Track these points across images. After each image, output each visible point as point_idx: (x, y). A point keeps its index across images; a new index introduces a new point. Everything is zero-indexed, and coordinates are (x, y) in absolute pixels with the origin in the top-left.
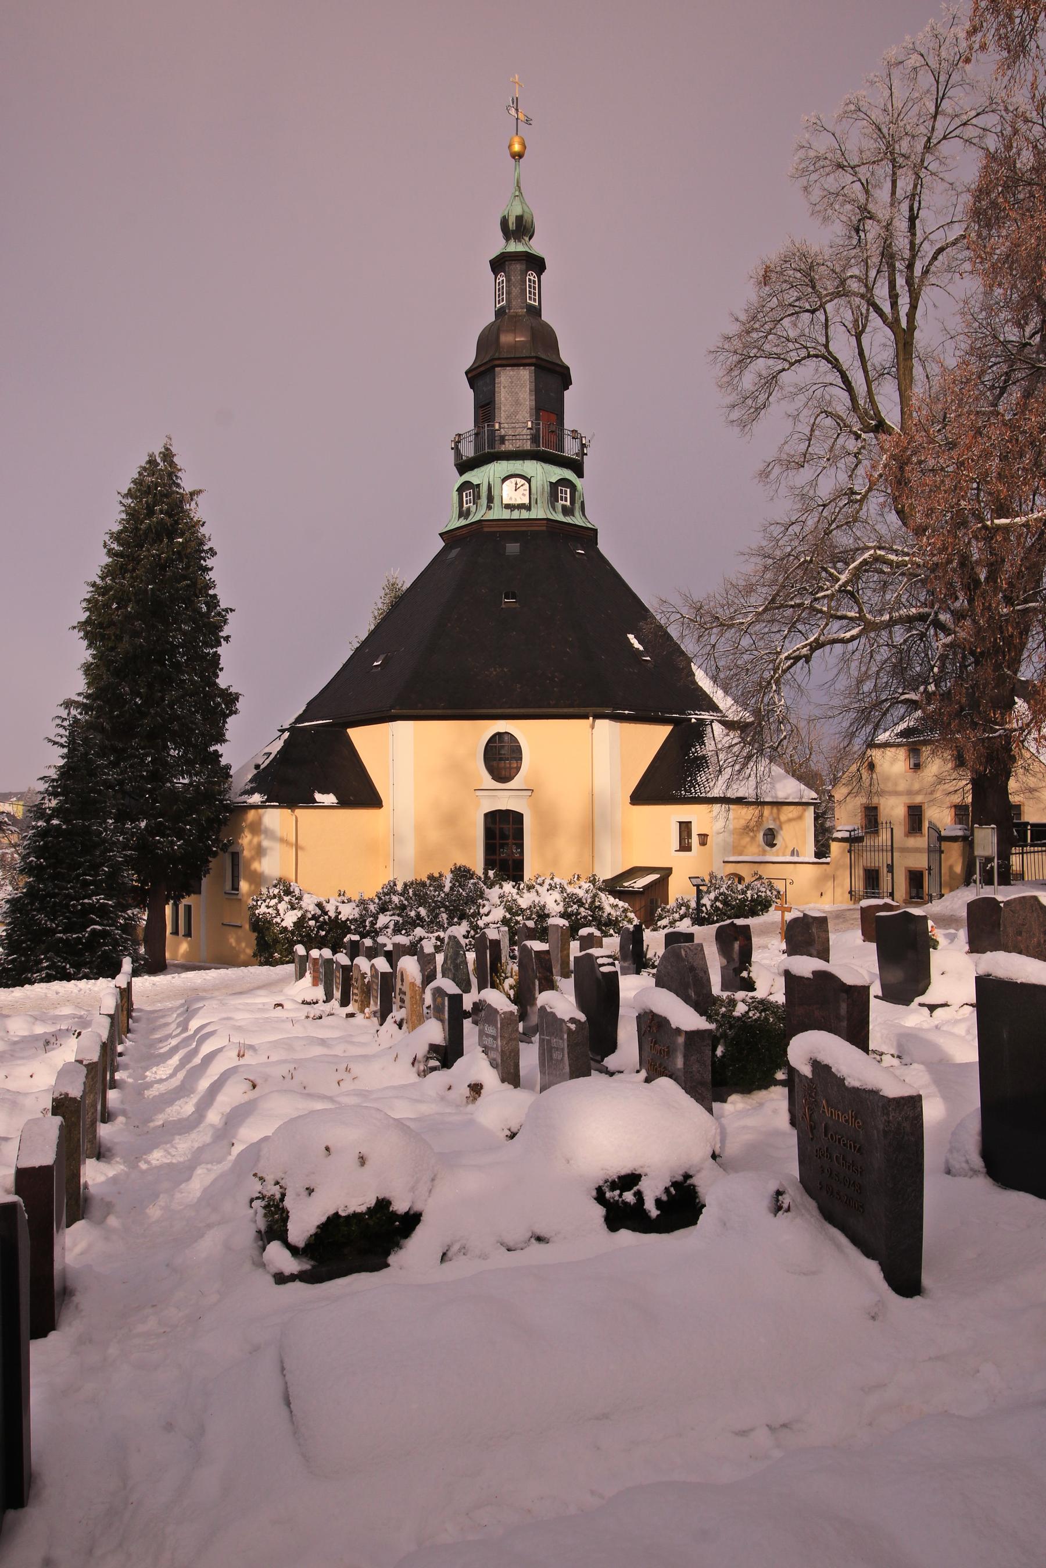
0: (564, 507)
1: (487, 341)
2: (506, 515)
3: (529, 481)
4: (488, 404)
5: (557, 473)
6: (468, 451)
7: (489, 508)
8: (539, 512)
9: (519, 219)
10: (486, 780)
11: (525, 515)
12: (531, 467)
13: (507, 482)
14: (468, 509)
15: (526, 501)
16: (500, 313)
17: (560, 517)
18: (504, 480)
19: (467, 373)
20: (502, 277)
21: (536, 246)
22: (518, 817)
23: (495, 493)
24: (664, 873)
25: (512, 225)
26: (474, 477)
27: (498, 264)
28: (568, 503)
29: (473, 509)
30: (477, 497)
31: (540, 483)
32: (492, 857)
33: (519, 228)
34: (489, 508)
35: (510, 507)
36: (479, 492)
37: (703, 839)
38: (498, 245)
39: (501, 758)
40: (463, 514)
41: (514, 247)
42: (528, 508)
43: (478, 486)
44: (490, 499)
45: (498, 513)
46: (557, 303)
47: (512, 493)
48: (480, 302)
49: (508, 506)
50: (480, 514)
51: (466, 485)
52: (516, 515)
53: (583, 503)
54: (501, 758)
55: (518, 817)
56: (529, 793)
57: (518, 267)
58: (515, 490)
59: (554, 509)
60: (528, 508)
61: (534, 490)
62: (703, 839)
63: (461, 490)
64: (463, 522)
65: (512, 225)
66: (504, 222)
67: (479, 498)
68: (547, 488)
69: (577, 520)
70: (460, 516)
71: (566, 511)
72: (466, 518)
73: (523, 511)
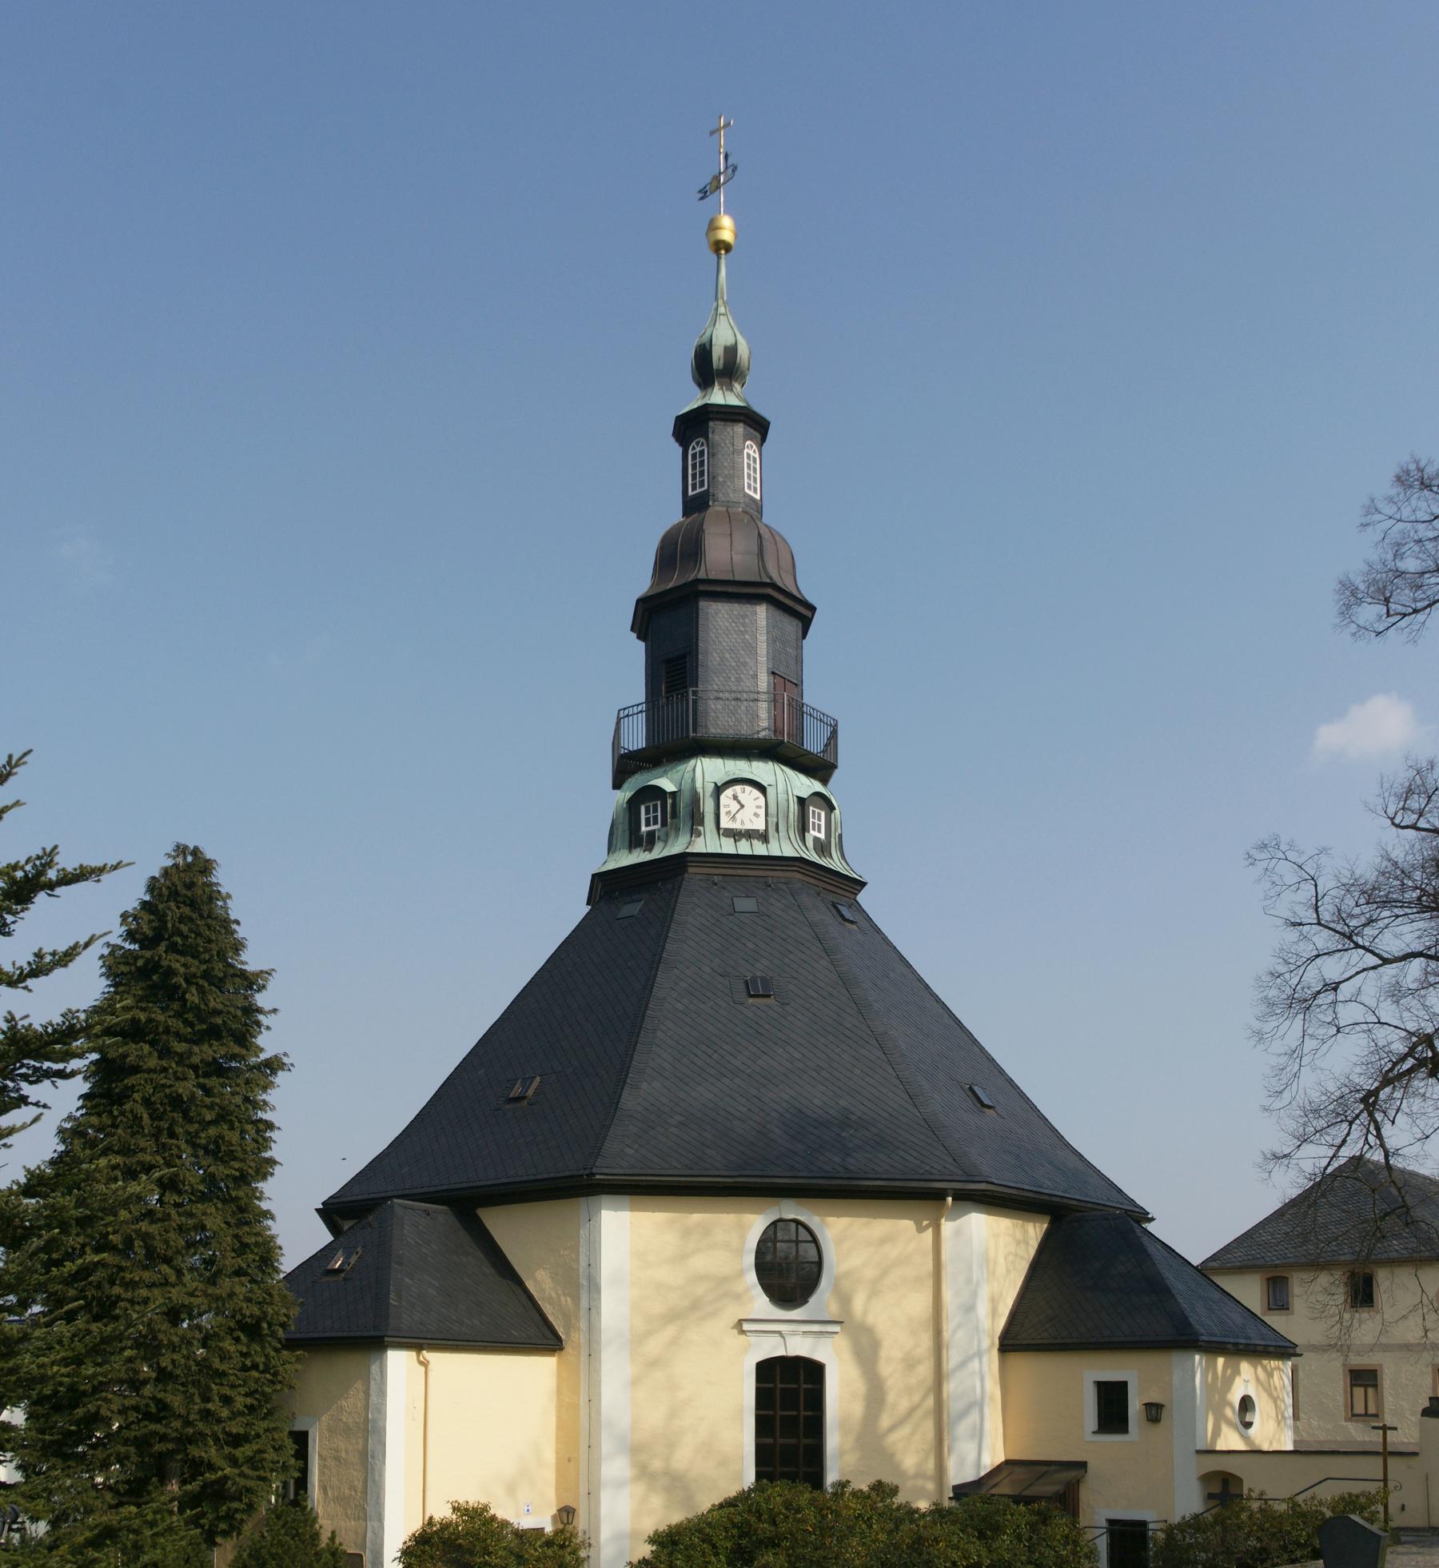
0: (816, 839)
1: (678, 551)
2: (728, 847)
3: (762, 789)
4: (684, 656)
5: (805, 785)
7: (694, 833)
8: (783, 847)
9: (731, 351)
11: (760, 849)
12: (763, 770)
13: (729, 792)
14: (651, 834)
15: (759, 825)
17: (814, 857)
18: (718, 790)
19: (638, 601)
23: (708, 807)
28: (822, 836)
32: (770, 1441)
35: (736, 835)
37: (1154, 1412)
41: (718, 396)
42: (764, 837)
45: (708, 843)
47: (745, 810)
52: (744, 848)
53: (840, 836)
58: (743, 806)
60: (764, 837)
61: (772, 809)
62: (1154, 1412)
66: (703, 354)
68: (794, 807)
69: (835, 863)
71: (822, 848)
72: (650, 847)
73: (755, 842)
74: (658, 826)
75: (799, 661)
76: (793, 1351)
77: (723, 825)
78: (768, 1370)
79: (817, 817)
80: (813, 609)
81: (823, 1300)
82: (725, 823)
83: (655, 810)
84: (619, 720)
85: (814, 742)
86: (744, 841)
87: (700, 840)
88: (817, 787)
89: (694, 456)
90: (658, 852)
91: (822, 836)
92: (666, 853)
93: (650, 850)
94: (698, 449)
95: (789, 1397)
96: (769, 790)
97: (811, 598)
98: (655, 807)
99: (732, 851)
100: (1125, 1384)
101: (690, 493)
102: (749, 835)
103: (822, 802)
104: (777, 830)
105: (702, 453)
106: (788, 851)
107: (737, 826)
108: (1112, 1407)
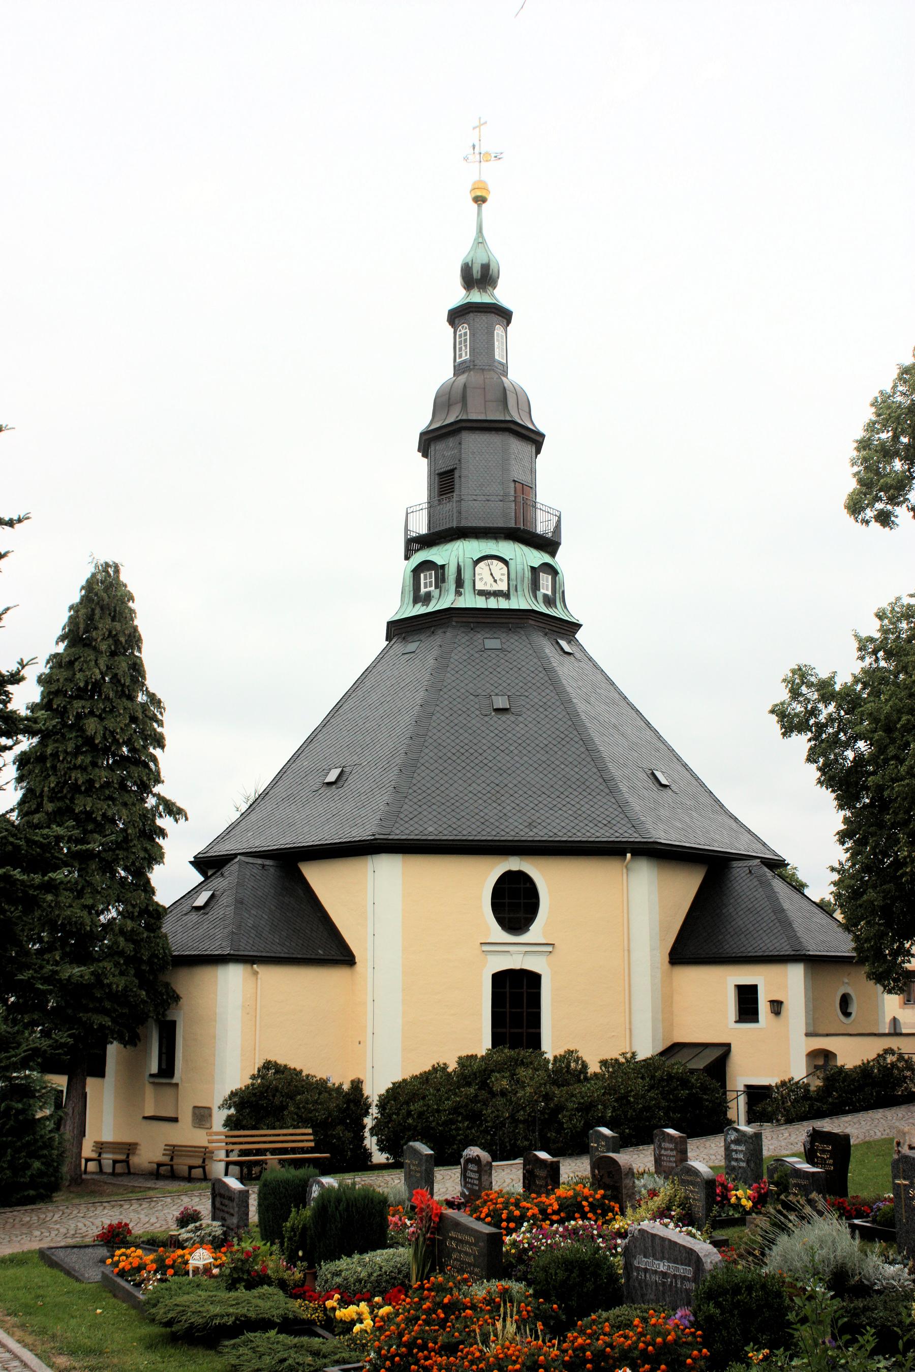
0: (545, 596)
2: (481, 603)
3: (505, 562)
5: (537, 558)
6: (420, 527)
7: (458, 593)
8: (520, 602)
10: (497, 933)
11: (503, 604)
12: (506, 549)
15: (503, 586)
16: (460, 369)
17: (543, 609)
19: (422, 434)
20: (464, 329)
21: (502, 295)
22: (532, 980)
23: (467, 576)
24: (725, 1048)
25: (476, 272)
26: (437, 555)
27: (456, 316)
28: (549, 593)
29: (436, 593)
30: (441, 580)
31: (519, 567)
33: (479, 276)
34: (458, 593)
36: (443, 574)
38: (458, 296)
39: (515, 904)
40: (419, 598)
41: (477, 297)
43: (443, 567)
44: (459, 583)
45: (469, 601)
46: (528, 361)
47: (491, 577)
48: (432, 361)
49: (482, 593)
50: (446, 601)
51: (426, 565)
52: (492, 603)
53: (563, 592)
54: (515, 904)
55: (532, 980)
56: (550, 949)
57: (482, 320)
58: (489, 573)
59: (536, 597)
60: (506, 595)
61: (513, 576)
63: (417, 571)
64: (420, 610)
65: (476, 272)
67: (443, 581)
68: (528, 574)
70: (415, 601)
71: (549, 601)
73: (500, 599)
74: (433, 588)
75: (533, 472)
76: (518, 967)
77: (477, 588)
78: (502, 980)
79: (545, 580)
80: (543, 436)
81: (536, 932)
82: (479, 586)
83: (431, 578)
84: (407, 514)
85: (543, 526)
86: (492, 598)
87: (461, 598)
88: (547, 558)
89: (460, 336)
90: (432, 607)
91: (549, 593)
92: (437, 608)
93: (427, 605)
94: (463, 331)
95: (516, 997)
96: (511, 562)
97: (541, 428)
98: (430, 575)
99: (484, 606)
100: (756, 986)
101: (458, 360)
102: (497, 594)
103: (550, 570)
104: (516, 590)
105: (465, 334)
106: (524, 606)
107: (487, 588)
108: (747, 1003)
